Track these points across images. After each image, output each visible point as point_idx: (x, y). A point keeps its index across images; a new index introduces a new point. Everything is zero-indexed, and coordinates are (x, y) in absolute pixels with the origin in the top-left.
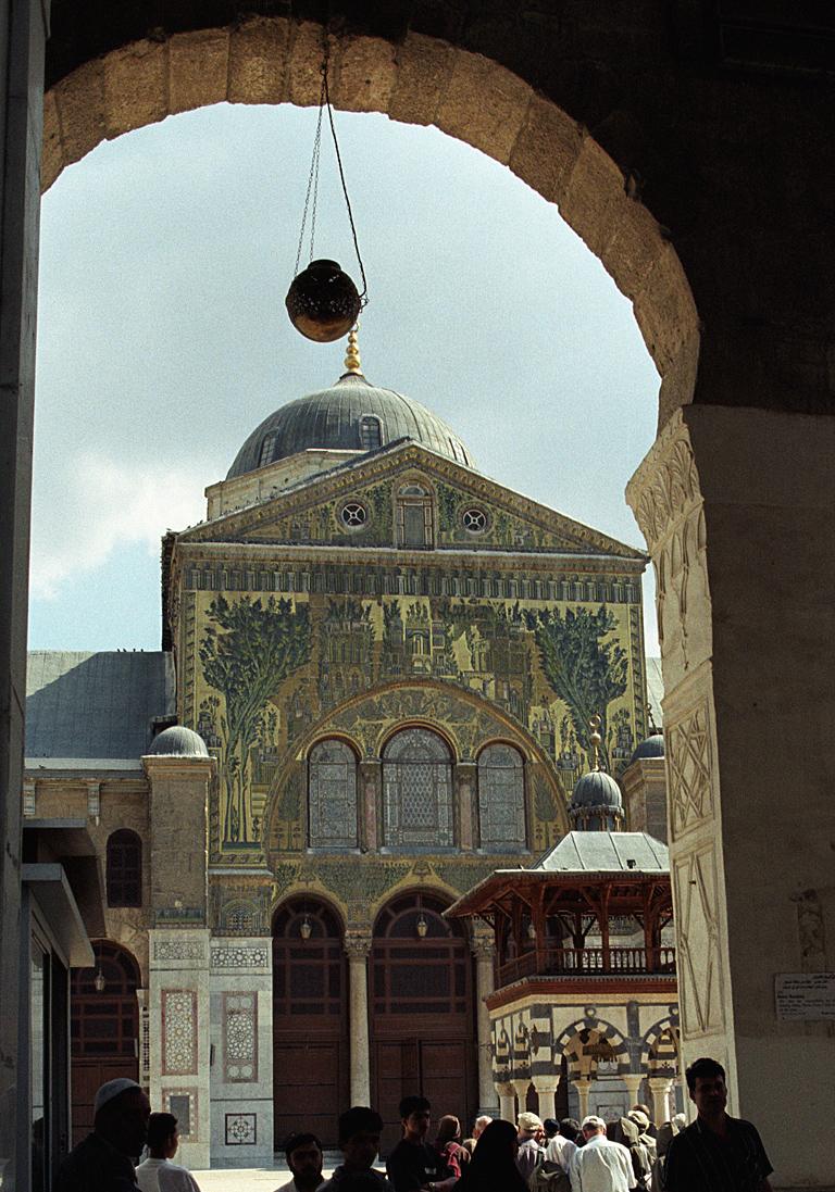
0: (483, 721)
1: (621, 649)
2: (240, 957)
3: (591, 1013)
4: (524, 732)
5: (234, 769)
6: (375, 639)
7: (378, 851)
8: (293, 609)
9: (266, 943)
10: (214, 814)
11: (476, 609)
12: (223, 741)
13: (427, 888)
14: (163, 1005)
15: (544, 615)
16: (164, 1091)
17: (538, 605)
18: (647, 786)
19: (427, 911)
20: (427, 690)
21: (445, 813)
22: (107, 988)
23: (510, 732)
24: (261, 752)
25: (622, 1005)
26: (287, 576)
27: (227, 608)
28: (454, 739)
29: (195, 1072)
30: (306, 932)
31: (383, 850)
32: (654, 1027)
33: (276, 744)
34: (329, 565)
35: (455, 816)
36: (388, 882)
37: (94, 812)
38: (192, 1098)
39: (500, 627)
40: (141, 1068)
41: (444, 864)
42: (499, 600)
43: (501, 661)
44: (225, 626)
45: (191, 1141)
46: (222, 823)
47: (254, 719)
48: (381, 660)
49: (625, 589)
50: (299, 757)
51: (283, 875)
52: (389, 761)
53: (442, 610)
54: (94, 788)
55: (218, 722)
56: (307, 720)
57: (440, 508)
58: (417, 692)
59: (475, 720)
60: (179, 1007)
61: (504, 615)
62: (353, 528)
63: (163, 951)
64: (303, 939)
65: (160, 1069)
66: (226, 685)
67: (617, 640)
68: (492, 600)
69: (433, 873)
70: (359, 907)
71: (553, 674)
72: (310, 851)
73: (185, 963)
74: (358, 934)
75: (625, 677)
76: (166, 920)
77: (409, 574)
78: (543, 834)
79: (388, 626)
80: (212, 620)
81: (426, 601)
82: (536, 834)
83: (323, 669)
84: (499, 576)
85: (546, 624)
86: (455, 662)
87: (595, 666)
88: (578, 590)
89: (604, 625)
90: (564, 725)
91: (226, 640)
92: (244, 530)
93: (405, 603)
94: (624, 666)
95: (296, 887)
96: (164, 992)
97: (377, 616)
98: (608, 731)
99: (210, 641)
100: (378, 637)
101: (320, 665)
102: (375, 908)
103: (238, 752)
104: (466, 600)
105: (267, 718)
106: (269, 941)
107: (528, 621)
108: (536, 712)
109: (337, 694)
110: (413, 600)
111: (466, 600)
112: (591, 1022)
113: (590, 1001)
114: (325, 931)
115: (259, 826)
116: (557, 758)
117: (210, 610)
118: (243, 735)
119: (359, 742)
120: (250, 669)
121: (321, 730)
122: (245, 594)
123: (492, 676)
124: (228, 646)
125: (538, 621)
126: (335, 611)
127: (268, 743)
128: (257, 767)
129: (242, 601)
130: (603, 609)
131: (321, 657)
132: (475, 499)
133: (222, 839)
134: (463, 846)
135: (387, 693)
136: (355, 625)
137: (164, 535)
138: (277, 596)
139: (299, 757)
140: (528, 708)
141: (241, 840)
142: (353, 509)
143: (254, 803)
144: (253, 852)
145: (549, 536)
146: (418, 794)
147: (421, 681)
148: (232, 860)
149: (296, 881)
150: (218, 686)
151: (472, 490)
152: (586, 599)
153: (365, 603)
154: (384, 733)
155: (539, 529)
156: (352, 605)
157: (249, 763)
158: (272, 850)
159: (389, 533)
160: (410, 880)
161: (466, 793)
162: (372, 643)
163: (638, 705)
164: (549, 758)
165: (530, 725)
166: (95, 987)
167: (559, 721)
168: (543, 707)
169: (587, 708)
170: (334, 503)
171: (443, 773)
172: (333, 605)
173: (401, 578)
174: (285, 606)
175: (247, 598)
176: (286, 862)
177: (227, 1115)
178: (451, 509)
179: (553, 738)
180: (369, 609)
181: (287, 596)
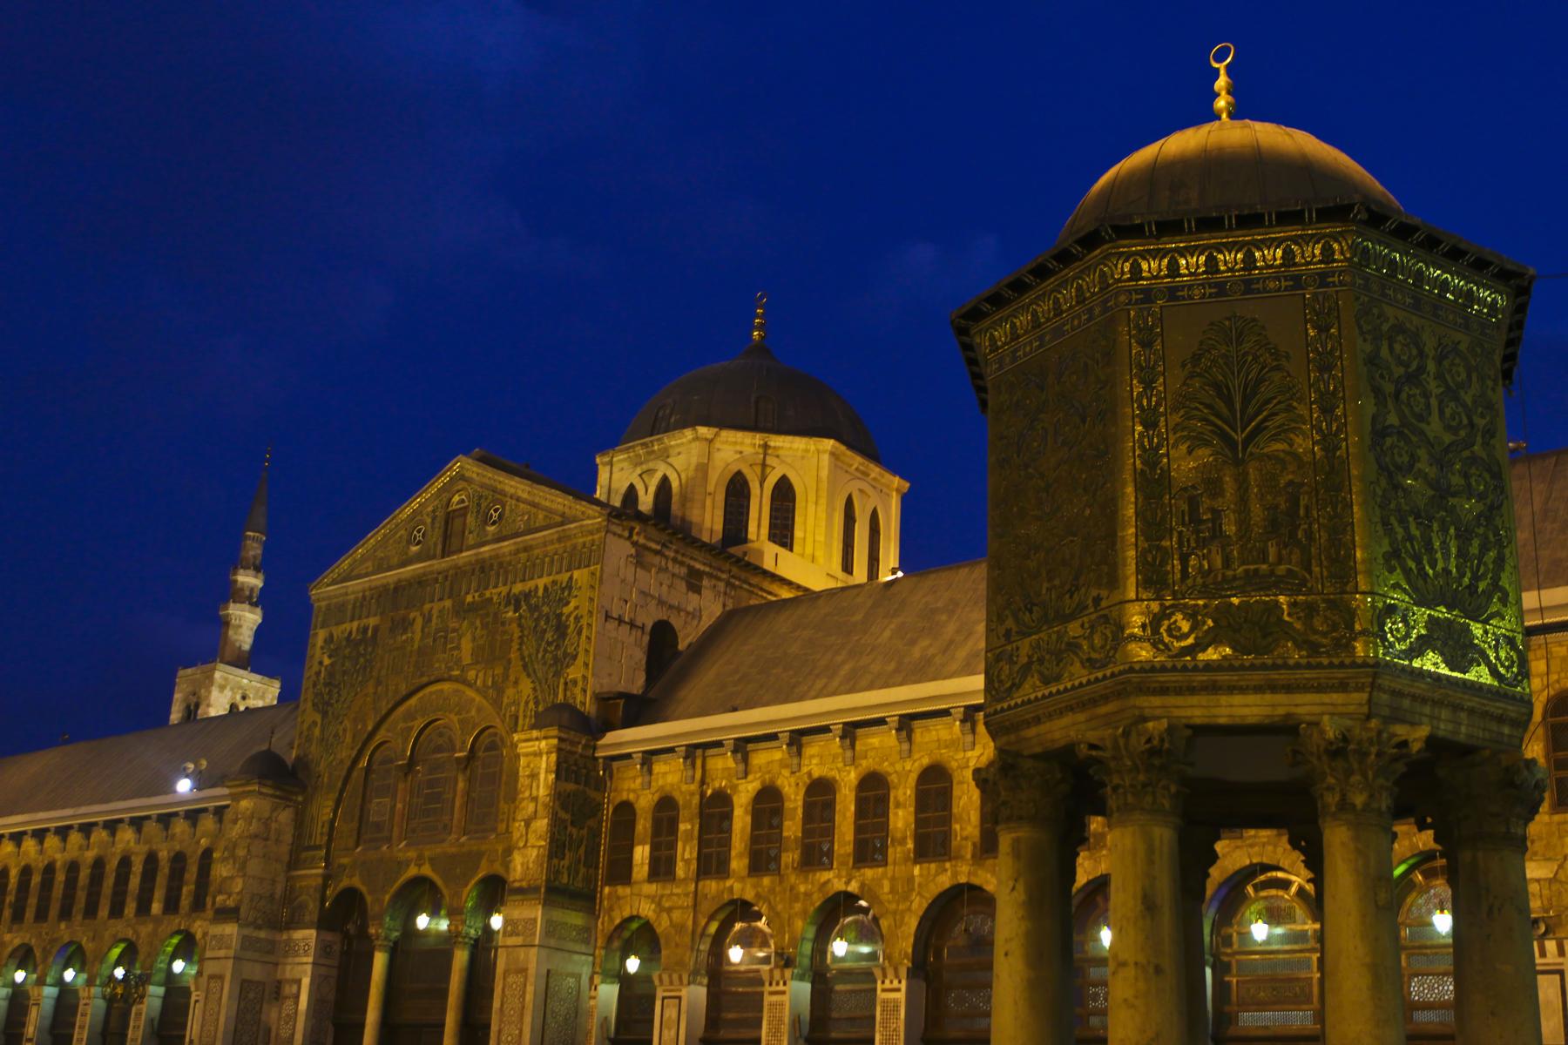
15: (527, 595)
20: (446, 687)
73: (222, 953)
83: (379, 683)
90: (527, 703)
94: (579, 633)
95: (345, 883)
108: (510, 692)
130: (571, 578)
156: (404, 619)
160: (413, 871)
161: (461, 785)
174: (366, 629)
176: (345, 861)
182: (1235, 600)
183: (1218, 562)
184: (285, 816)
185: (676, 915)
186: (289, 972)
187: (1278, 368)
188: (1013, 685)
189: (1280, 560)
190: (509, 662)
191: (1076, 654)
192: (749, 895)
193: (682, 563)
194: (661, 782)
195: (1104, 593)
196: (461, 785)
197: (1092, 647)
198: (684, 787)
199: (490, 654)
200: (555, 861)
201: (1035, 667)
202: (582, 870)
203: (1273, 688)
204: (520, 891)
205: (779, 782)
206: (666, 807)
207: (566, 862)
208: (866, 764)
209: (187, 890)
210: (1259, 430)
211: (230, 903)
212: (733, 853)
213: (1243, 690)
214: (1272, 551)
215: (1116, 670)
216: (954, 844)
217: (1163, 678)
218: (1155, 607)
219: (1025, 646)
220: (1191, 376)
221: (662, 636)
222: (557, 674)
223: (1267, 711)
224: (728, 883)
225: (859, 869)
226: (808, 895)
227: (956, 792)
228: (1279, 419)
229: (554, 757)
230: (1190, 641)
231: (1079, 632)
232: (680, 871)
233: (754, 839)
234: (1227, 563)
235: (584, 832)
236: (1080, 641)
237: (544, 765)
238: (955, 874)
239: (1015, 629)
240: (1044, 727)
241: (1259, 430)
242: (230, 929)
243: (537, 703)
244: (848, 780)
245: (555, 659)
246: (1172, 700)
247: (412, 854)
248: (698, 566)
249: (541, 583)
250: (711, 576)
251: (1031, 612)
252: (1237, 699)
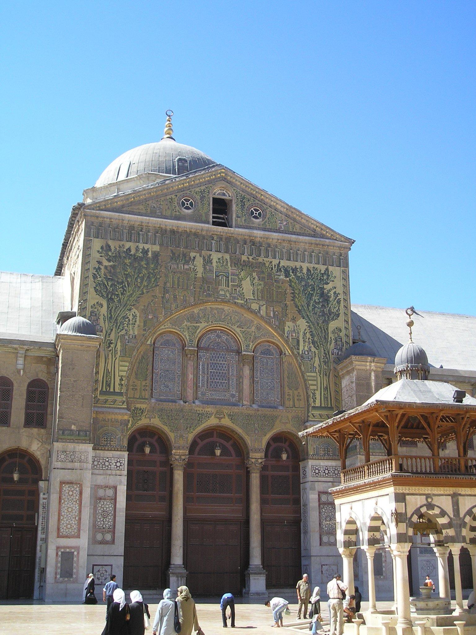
0: (258, 328)
1: (337, 293)
2: (107, 464)
3: (429, 500)
4: (282, 336)
5: (110, 346)
6: (197, 276)
7: (194, 403)
8: (150, 254)
9: (124, 455)
10: (97, 373)
11: (256, 263)
12: (104, 329)
13: (223, 427)
14: (61, 491)
15: (295, 270)
16: (58, 548)
17: (292, 264)
18: (355, 373)
19: (222, 441)
21: (233, 382)
22: (21, 480)
23: (273, 336)
24: (127, 337)
25: (449, 495)
26: (147, 235)
27: (110, 250)
28: (241, 339)
29: (78, 536)
30: (147, 450)
31: (197, 402)
32: (468, 510)
33: (136, 333)
34: (173, 232)
35: (239, 384)
36: (200, 421)
37: (20, 367)
38: (75, 553)
39: (270, 276)
40: (39, 532)
41: (233, 412)
42: (270, 259)
43: (270, 294)
44: (109, 260)
45: (73, 582)
46: (100, 378)
47: (123, 317)
48: (201, 288)
49: (340, 259)
50: (149, 342)
51: (136, 413)
52: (202, 348)
53: (236, 262)
54: (22, 352)
55: (102, 317)
56: (155, 320)
57: (237, 205)
58: (220, 309)
59: (253, 328)
60: (71, 493)
61: (272, 268)
62: (186, 211)
63: (63, 456)
64: (145, 455)
65: (55, 534)
66: (108, 295)
67: (335, 288)
68: (264, 259)
69: (226, 417)
70: (181, 436)
71: (299, 304)
72: (153, 401)
73: (77, 465)
74: (180, 453)
75: (339, 308)
76: (66, 437)
77: (218, 240)
78: (291, 397)
79: (205, 268)
80: (101, 256)
82: (287, 397)
83: (166, 291)
84: (269, 245)
85: (295, 275)
86: (243, 293)
87: (322, 302)
88: (313, 257)
89: (328, 279)
90: (305, 334)
91: (109, 268)
92: (123, 206)
93: (215, 256)
94: (339, 302)
95: (144, 422)
96: (62, 483)
97: (199, 262)
98: (329, 339)
99: (99, 268)
100: (199, 275)
101: (164, 288)
102: (191, 437)
103: (113, 336)
104: (251, 259)
105: (131, 317)
106: (126, 454)
107: (285, 273)
109: (174, 306)
110: (220, 255)
111: (251, 258)
112: (430, 506)
113: (429, 492)
114: (158, 451)
115: (123, 382)
116: (301, 353)
117: (100, 251)
118: (116, 326)
119: (185, 336)
120: (122, 287)
121: (163, 327)
122: (122, 243)
123: (264, 303)
124: (110, 272)
125: (291, 273)
126: (174, 257)
127: (131, 332)
128: (124, 346)
129: (120, 247)
130: (327, 269)
131: (165, 283)
132: (257, 201)
133: (100, 389)
134: (244, 402)
135: (202, 308)
136: (186, 267)
137: (76, 204)
138: (141, 246)
139: (149, 342)
140: (284, 323)
141: (112, 390)
142: (187, 200)
143: (121, 368)
144: (119, 398)
145: (297, 226)
146: (218, 370)
147: (224, 301)
148: (106, 402)
149: (143, 418)
150: (102, 296)
151: (255, 198)
152: (318, 263)
154: (200, 331)
155: (292, 221)
156: (184, 255)
157: (119, 344)
158: (130, 398)
159: (207, 215)
160: (213, 421)
161: (247, 371)
162: (195, 278)
163: (346, 326)
164: (296, 353)
165: (286, 333)
166: (13, 478)
167: (302, 332)
168: (293, 322)
169: (318, 325)
170: (176, 196)
171: (233, 358)
172: (174, 254)
173: (214, 242)
174: (145, 252)
175: (123, 245)
176: (138, 406)
177: (94, 565)
178: (243, 206)
179: (298, 341)
180: (194, 258)
181: (146, 246)
222: (326, 322)
245: (324, 314)
247: (210, 409)
249: (305, 266)
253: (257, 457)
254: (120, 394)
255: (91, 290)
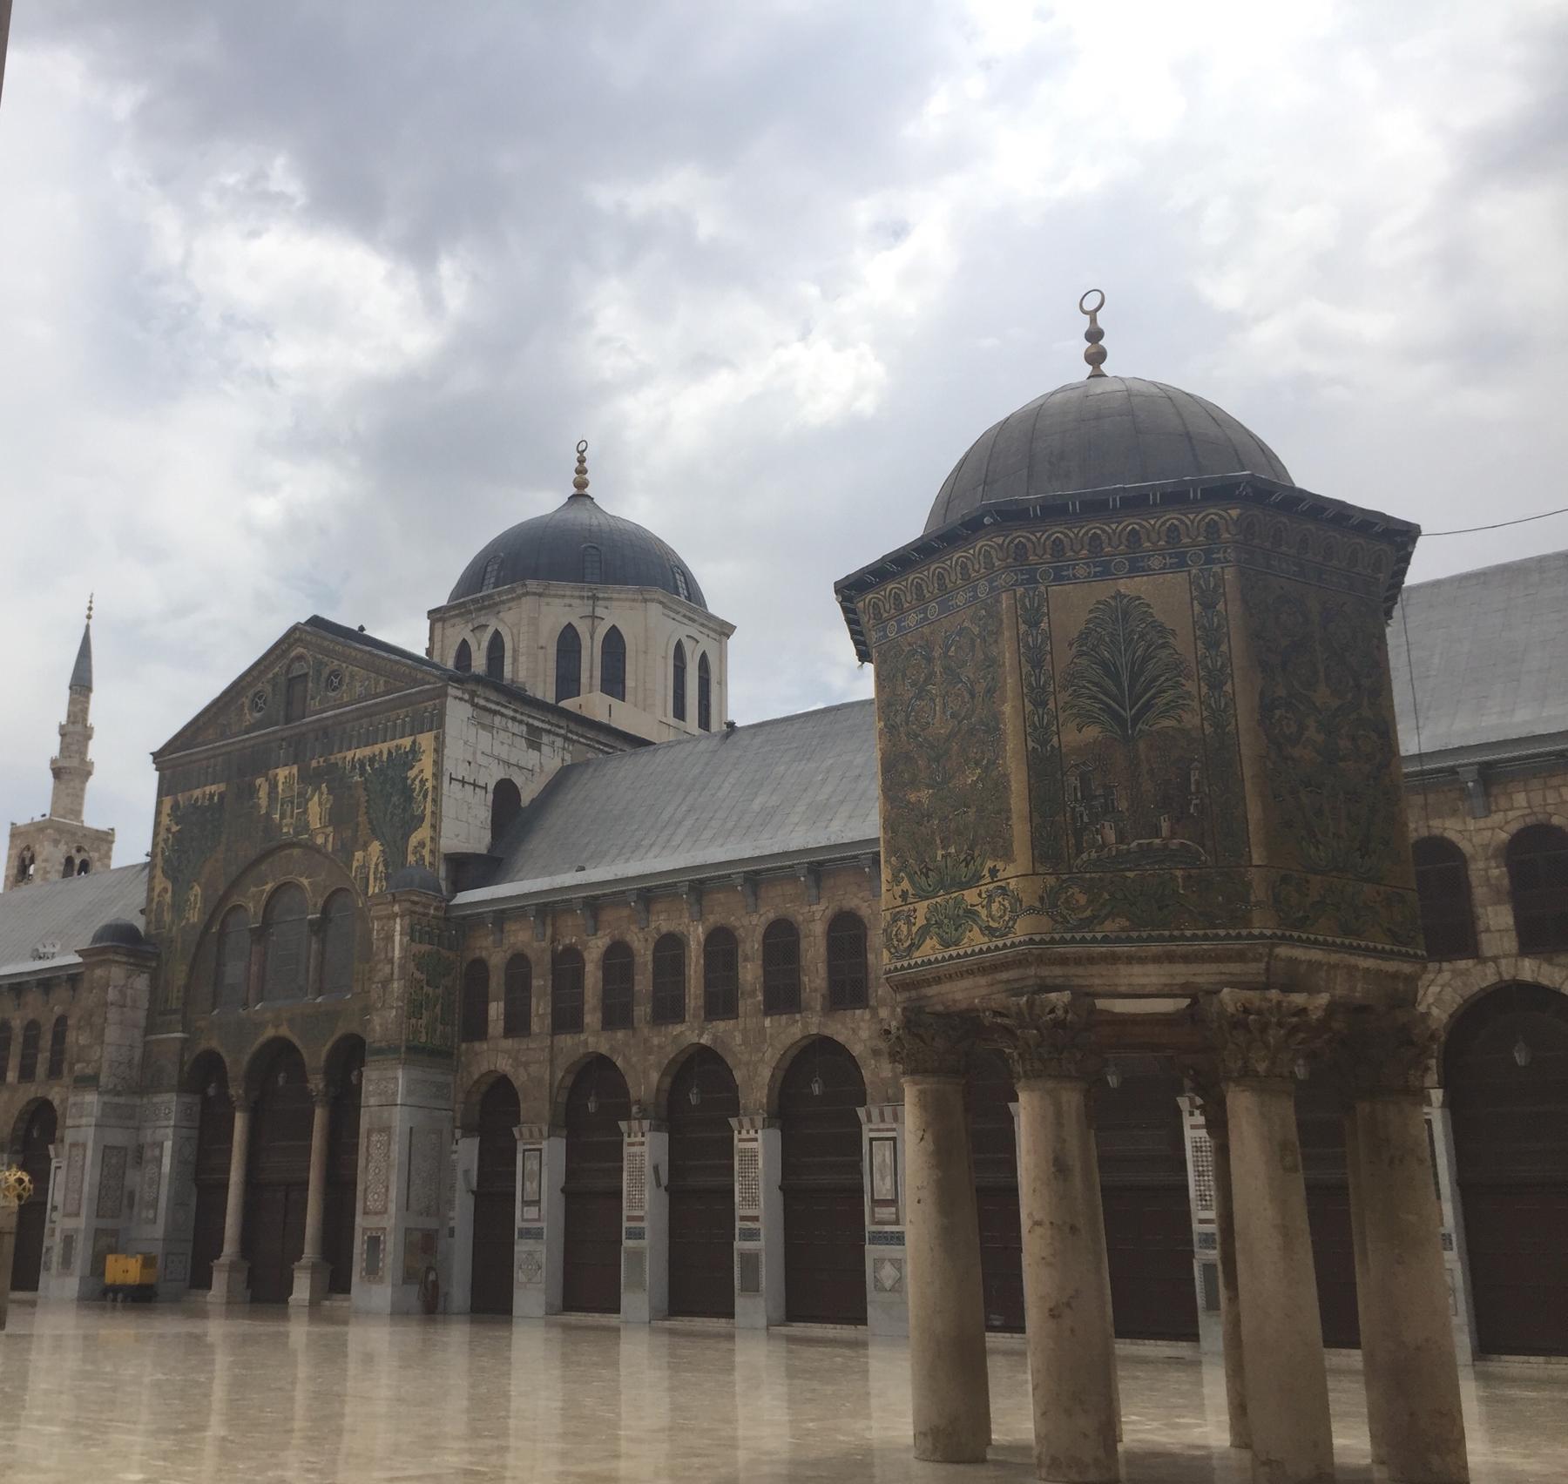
15: (372, 760)
17: (367, 751)
20: (296, 852)
29: (77, 1215)
81: (295, 770)
94: (425, 796)
95: (203, 1045)
97: (263, 794)
102: (246, 1058)
108: (359, 855)
138: (208, 789)
153: (258, 781)
160: (270, 1032)
161: (314, 946)
174: (212, 796)
182: (1131, 874)
183: (1111, 837)
184: (141, 982)
185: (533, 1069)
186: (148, 1136)
187: (1164, 646)
188: (912, 945)
189: (1173, 835)
190: (358, 824)
191: (974, 921)
192: (604, 1049)
193: (521, 722)
194: (512, 940)
195: (1000, 865)
196: (314, 946)
197: (990, 915)
198: (535, 944)
199: (336, 818)
200: (413, 1021)
201: (934, 929)
202: (440, 1028)
203: (1171, 958)
204: (380, 1051)
205: (628, 938)
206: (519, 965)
207: (423, 1022)
208: (713, 919)
209: (43, 1057)
210: (1148, 706)
211: (89, 1071)
212: (586, 1007)
213: (1142, 960)
214: (1165, 826)
215: (1017, 940)
216: (804, 996)
217: (1061, 949)
218: (1051, 880)
219: (922, 907)
220: (1081, 654)
221: (505, 792)
222: (406, 837)
223: (1163, 980)
224: (583, 1037)
225: (711, 1021)
226: (660, 1047)
227: (804, 944)
228: (1169, 696)
229: (407, 920)
230: (1088, 913)
231: (976, 900)
232: (535, 1028)
233: (606, 994)
234: (1121, 838)
235: (440, 991)
236: (978, 908)
237: (398, 928)
238: (806, 1025)
239: (911, 891)
240: (945, 988)
241: (1148, 706)
242: (91, 1098)
243: (386, 865)
244: (696, 935)
246: (1071, 970)
248: (536, 723)
250: (549, 732)
251: (927, 877)
252: (1137, 969)
253: (317, 1083)
254: (175, 1012)
255: (159, 872)
